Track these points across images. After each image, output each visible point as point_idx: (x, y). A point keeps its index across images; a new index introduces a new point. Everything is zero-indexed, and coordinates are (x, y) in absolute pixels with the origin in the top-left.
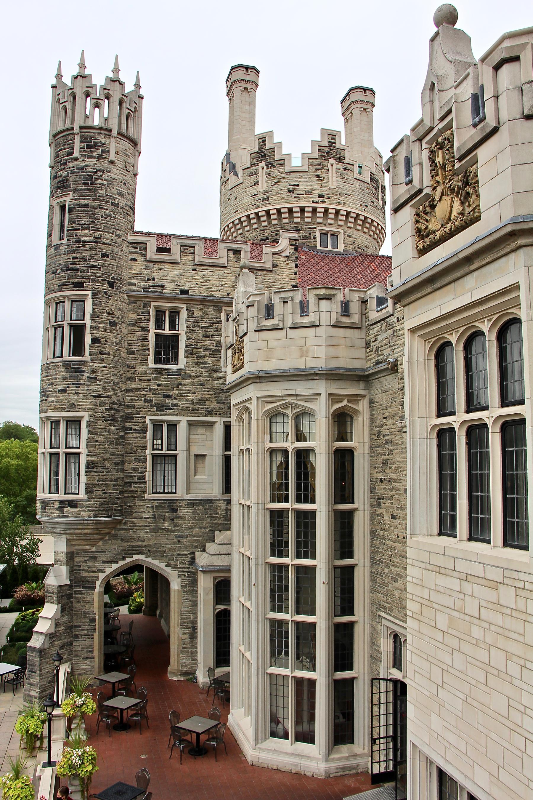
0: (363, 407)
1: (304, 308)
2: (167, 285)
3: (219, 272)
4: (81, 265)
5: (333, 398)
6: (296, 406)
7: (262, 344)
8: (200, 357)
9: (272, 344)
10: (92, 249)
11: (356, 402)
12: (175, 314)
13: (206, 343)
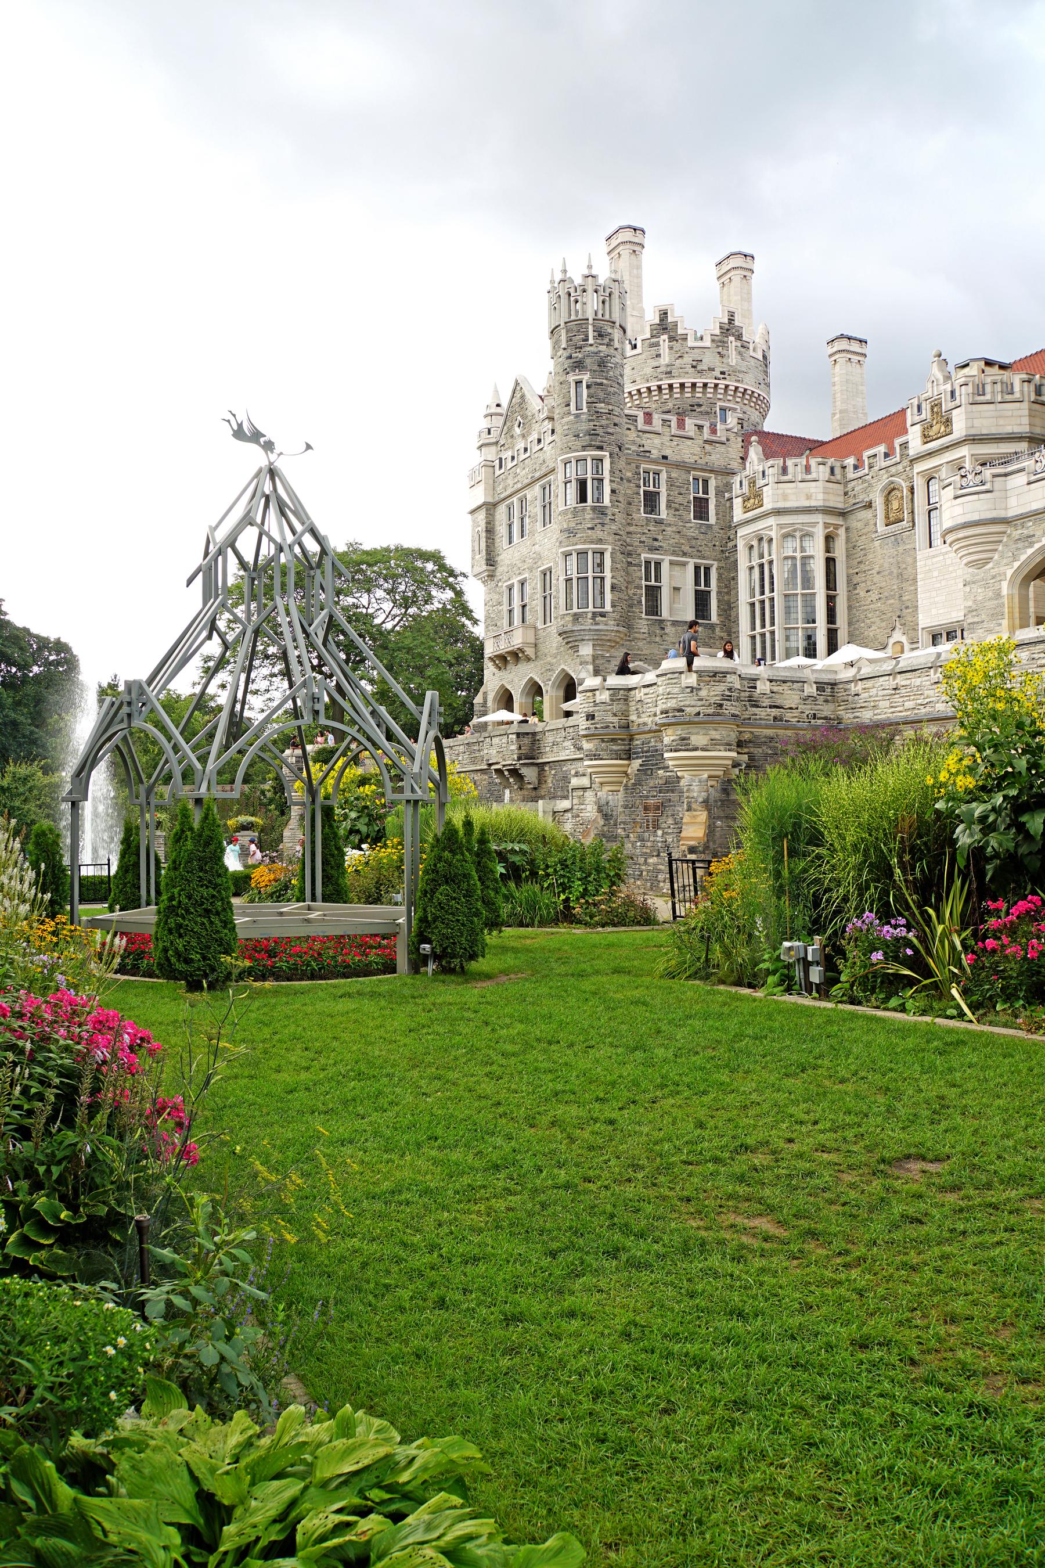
0: (842, 532)
1: (808, 469)
2: (653, 451)
3: (689, 442)
4: (600, 431)
5: (826, 525)
6: (801, 530)
7: (780, 492)
8: (677, 510)
9: (787, 491)
10: (607, 419)
11: (837, 529)
12: (657, 473)
13: (680, 499)
